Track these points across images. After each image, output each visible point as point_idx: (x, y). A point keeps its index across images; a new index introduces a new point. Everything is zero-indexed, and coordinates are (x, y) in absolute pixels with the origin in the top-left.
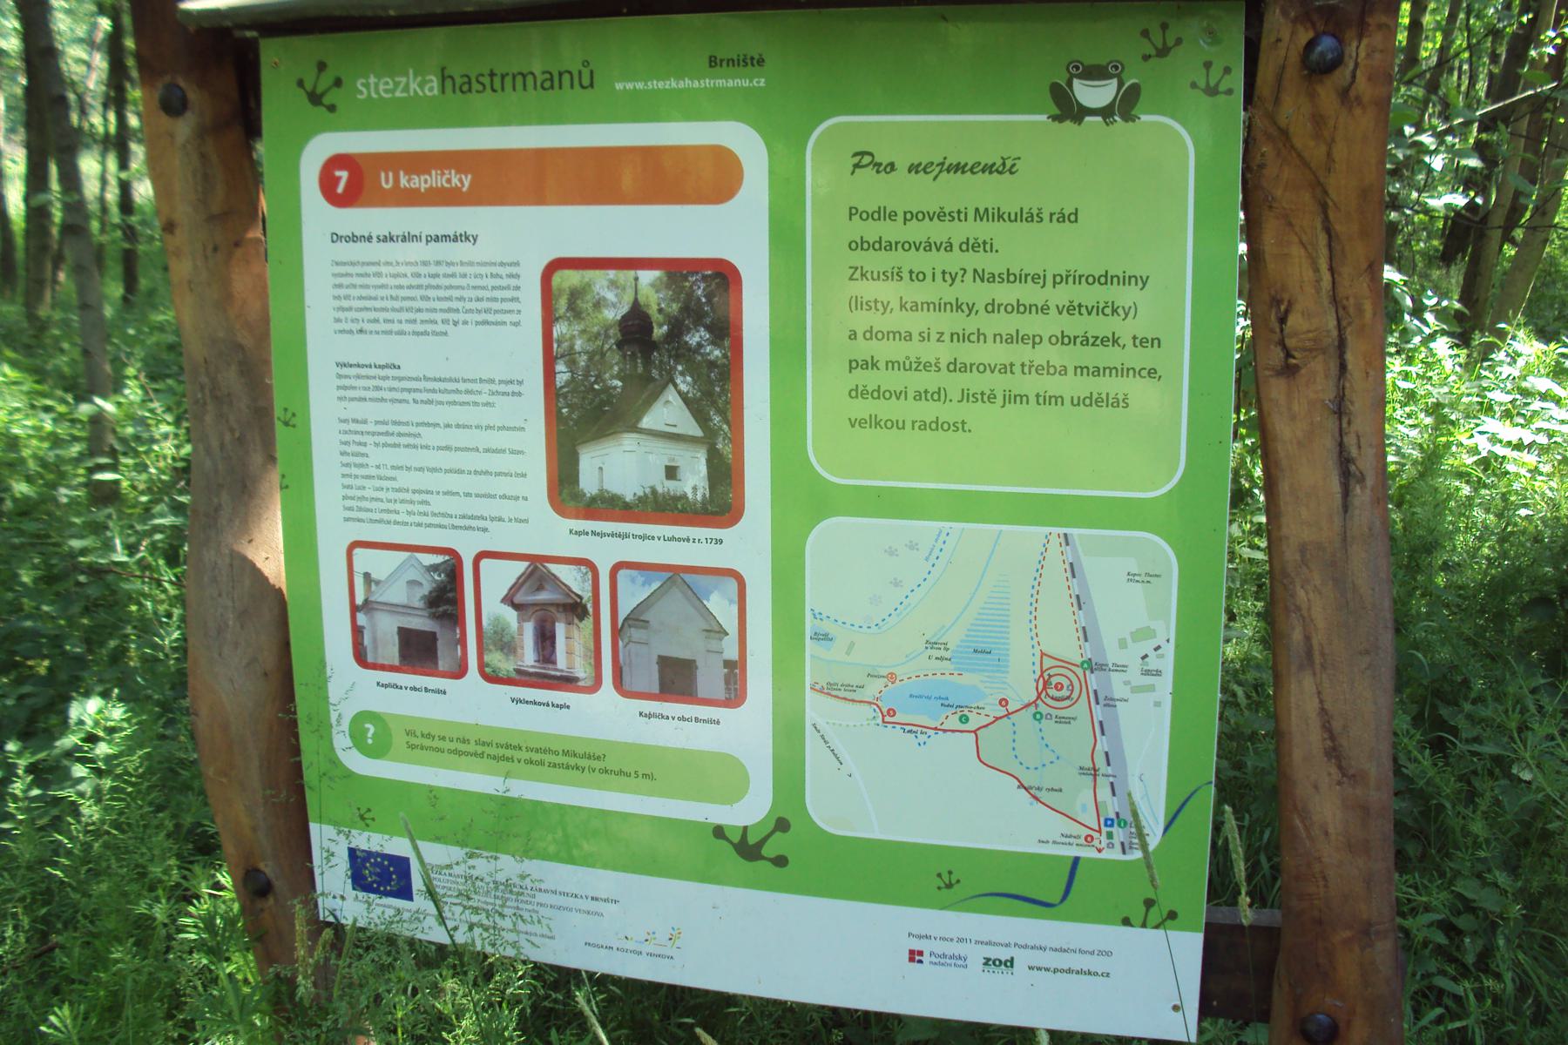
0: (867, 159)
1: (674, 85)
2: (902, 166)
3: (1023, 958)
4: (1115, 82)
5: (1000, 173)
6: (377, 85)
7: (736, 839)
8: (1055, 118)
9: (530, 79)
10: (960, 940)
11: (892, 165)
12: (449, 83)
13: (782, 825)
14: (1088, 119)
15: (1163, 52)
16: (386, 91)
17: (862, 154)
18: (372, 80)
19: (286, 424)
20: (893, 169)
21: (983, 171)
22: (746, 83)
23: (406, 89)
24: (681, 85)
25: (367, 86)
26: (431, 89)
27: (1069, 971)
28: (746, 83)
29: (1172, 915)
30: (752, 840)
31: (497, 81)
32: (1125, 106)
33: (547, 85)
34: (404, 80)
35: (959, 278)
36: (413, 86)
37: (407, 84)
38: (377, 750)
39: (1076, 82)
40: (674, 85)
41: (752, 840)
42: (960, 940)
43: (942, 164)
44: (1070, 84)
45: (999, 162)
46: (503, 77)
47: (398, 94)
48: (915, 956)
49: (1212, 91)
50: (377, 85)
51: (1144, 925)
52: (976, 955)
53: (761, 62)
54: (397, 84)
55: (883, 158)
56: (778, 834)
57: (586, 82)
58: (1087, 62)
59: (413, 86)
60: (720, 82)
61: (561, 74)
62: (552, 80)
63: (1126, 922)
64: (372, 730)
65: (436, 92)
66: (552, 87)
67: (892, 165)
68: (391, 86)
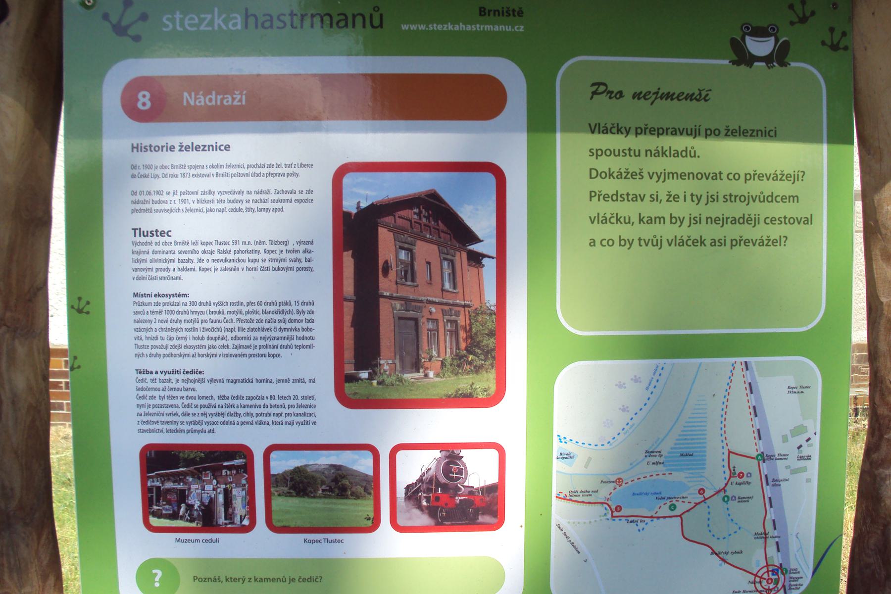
0: (602, 88)
1: (450, 27)
2: (628, 94)
4: (773, 38)
5: (698, 100)
8: (734, 62)
11: (621, 93)
12: (252, 20)
14: (756, 64)
15: (803, 20)
16: (191, 25)
17: (599, 84)
18: (178, 16)
21: (686, 99)
22: (508, 29)
23: (211, 23)
24: (457, 28)
25: (173, 20)
26: (235, 25)
28: (508, 29)
32: (780, 56)
34: (209, 17)
35: (662, 178)
36: (218, 21)
39: (747, 38)
40: (450, 27)
43: (657, 93)
44: (743, 39)
45: (697, 92)
47: (202, 28)
54: (202, 20)
57: (376, 22)
58: (754, 25)
60: (488, 27)
61: (354, 16)
65: (239, 27)
66: (346, 25)
67: (621, 93)
68: (197, 21)
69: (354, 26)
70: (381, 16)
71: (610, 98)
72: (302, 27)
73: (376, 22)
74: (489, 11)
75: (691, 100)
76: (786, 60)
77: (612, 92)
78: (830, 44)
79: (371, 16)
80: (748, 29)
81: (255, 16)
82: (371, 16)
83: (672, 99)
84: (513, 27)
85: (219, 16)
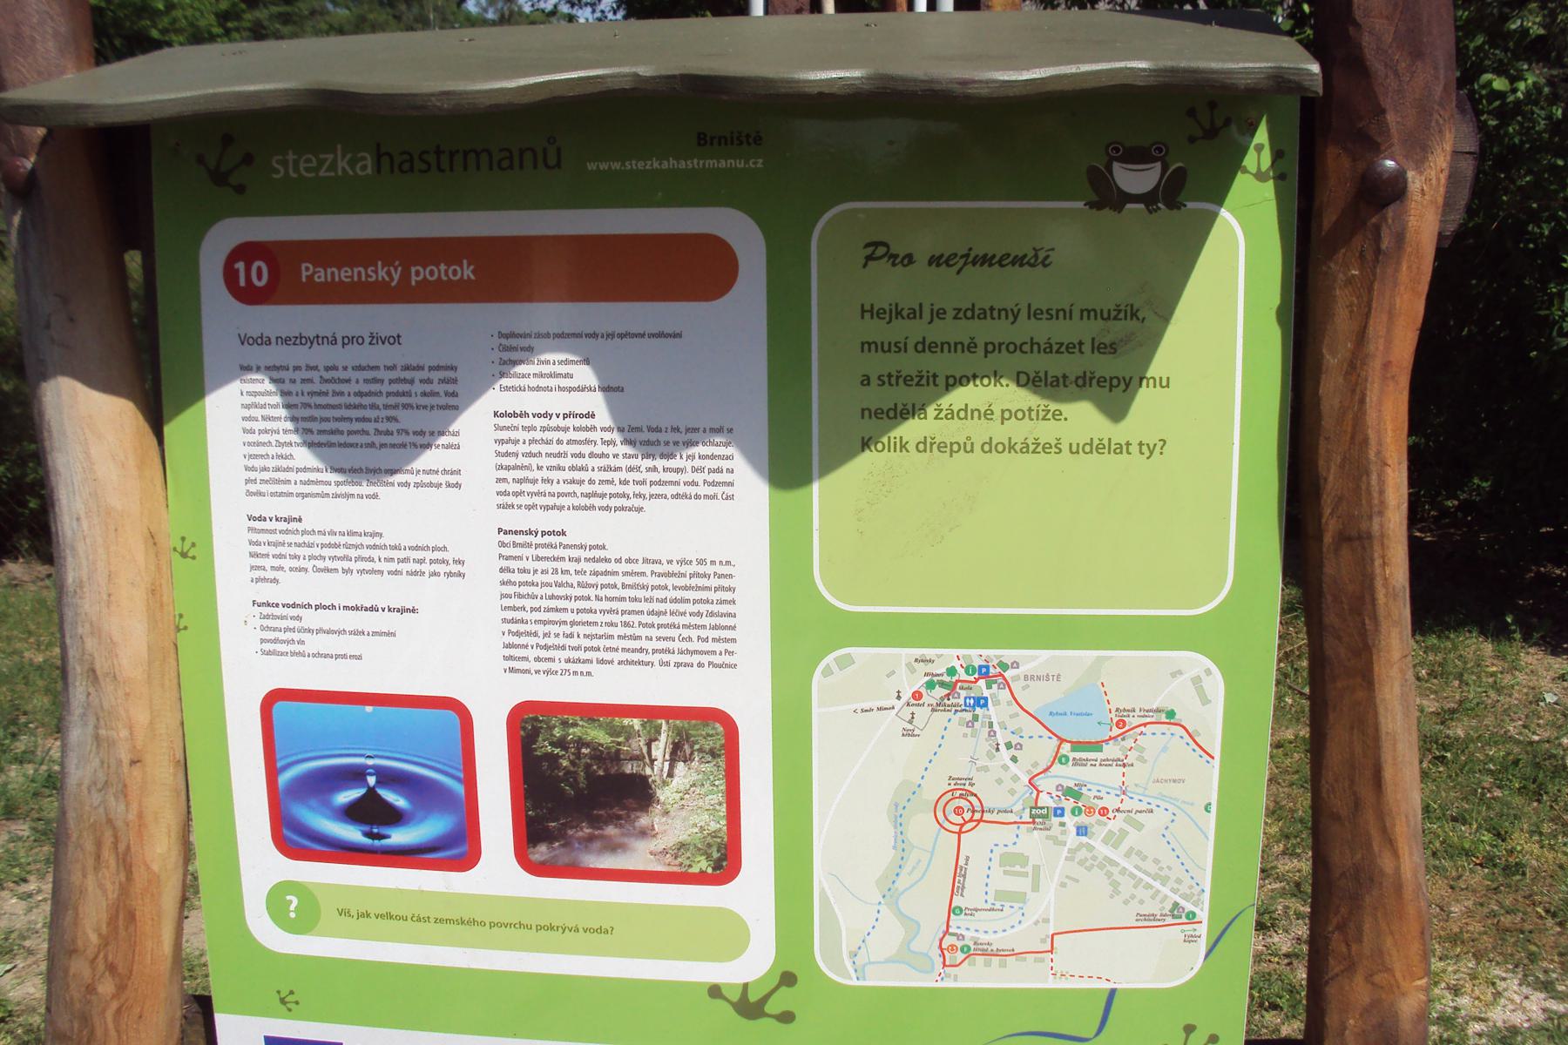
0: (881, 251)
1: (656, 165)
2: (921, 258)
4: (1158, 165)
6: (296, 163)
7: (735, 997)
9: (484, 157)
12: (385, 161)
13: (788, 979)
14: (1129, 206)
16: (307, 170)
17: (876, 244)
18: (291, 157)
20: (911, 262)
22: (740, 164)
23: (333, 167)
24: (665, 165)
25: (285, 163)
26: (364, 168)
28: (740, 164)
31: (445, 159)
33: (505, 164)
34: (331, 156)
36: (342, 164)
37: (335, 161)
38: (304, 923)
39: (1116, 166)
40: (656, 165)
41: (753, 997)
43: (967, 256)
45: (1031, 254)
46: (452, 155)
47: (322, 173)
50: (296, 163)
53: (758, 140)
54: (321, 163)
55: (899, 249)
56: (783, 989)
57: (552, 161)
59: (342, 164)
62: (511, 158)
65: (369, 171)
66: (511, 167)
68: (314, 164)
69: (521, 166)
70: (559, 150)
71: (894, 265)
72: (451, 169)
73: (552, 161)
74: (712, 138)
75: (1021, 265)
76: (1180, 199)
77: (895, 256)
78: (1254, 170)
79: (545, 151)
80: (1117, 150)
81: (388, 154)
82: (545, 151)
83: (991, 265)
84: (747, 162)
85: (344, 156)
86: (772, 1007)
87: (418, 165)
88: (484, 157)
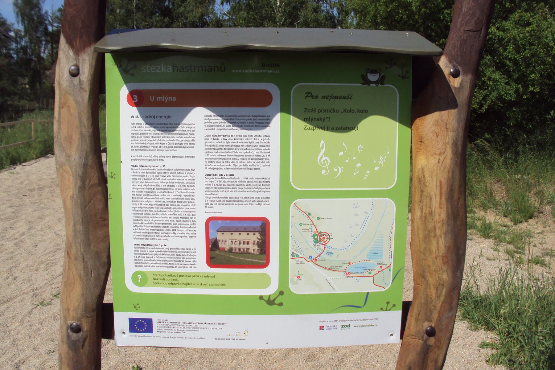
0: (310, 95)
3: (353, 324)
6: (149, 68)
7: (267, 299)
9: (204, 68)
10: (335, 321)
11: (317, 97)
13: (281, 293)
14: (371, 85)
16: (153, 70)
18: (148, 66)
19: (112, 177)
22: (274, 72)
23: (160, 69)
24: (254, 71)
26: (169, 70)
27: (366, 326)
28: (274, 72)
29: (394, 306)
30: (272, 299)
32: (381, 81)
33: (210, 70)
34: (160, 67)
39: (368, 74)
41: (272, 299)
42: (335, 321)
44: (367, 74)
47: (157, 71)
48: (321, 328)
49: (404, 77)
50: (149, 68)
51: (386, 310)
52: (339, 325)
53: (278, 66)
54: (157, 69)
57: (223, 69)
60: (266, 71)
63: (382, 309)
64: (140, 276)
67: (317, 97)
73: (223, 69)
86: (277, 302)
87: (185, 70)
88: (204, 68)
